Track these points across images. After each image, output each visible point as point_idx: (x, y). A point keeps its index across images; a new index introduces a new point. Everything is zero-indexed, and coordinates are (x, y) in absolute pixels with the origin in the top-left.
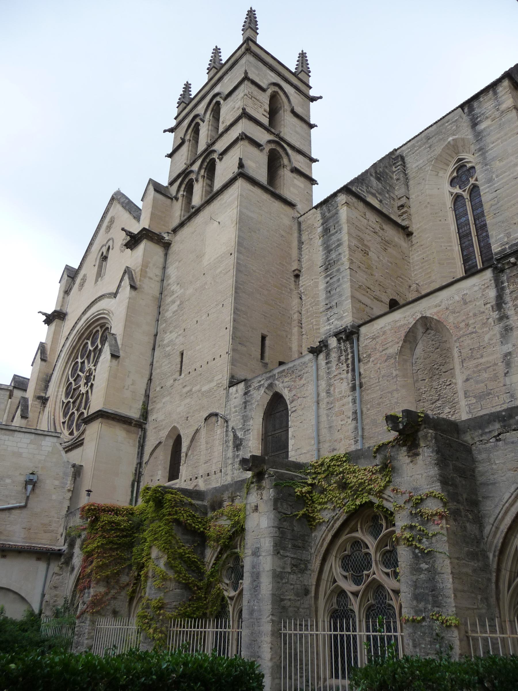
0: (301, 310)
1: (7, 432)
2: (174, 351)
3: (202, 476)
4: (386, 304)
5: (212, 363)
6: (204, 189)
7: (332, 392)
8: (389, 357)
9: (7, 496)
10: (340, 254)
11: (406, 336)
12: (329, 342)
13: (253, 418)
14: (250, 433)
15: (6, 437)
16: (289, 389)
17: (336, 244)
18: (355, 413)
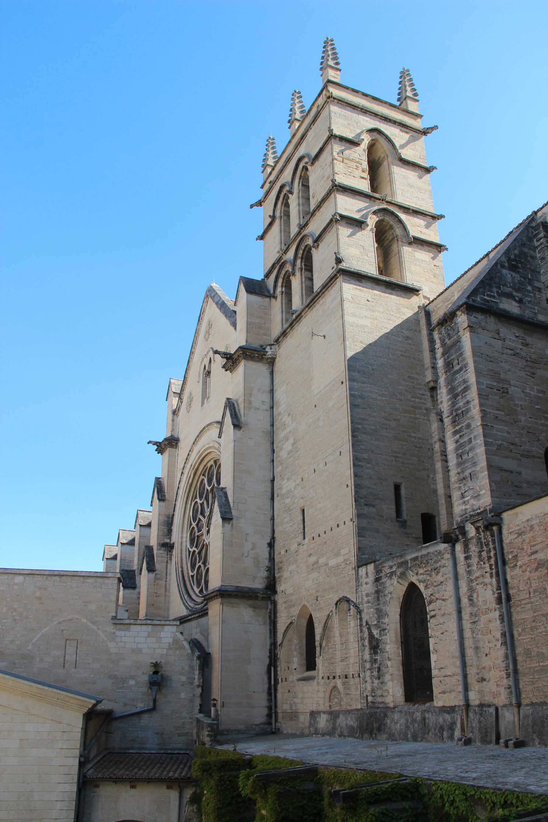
0: (444, 436)
1: (122, 627)
2: (295, 505)
4: (540, 458)
5: (336, 530)
6: (304, 285)
7: (475, 600)
9: (133, 700)
10: (468, 402)
12: (466, 528)
13: (388, 615)
14: (386, 635)
15: (122, 633)
16: (425, 584)
17: (463, 387)
18: (503, 635)
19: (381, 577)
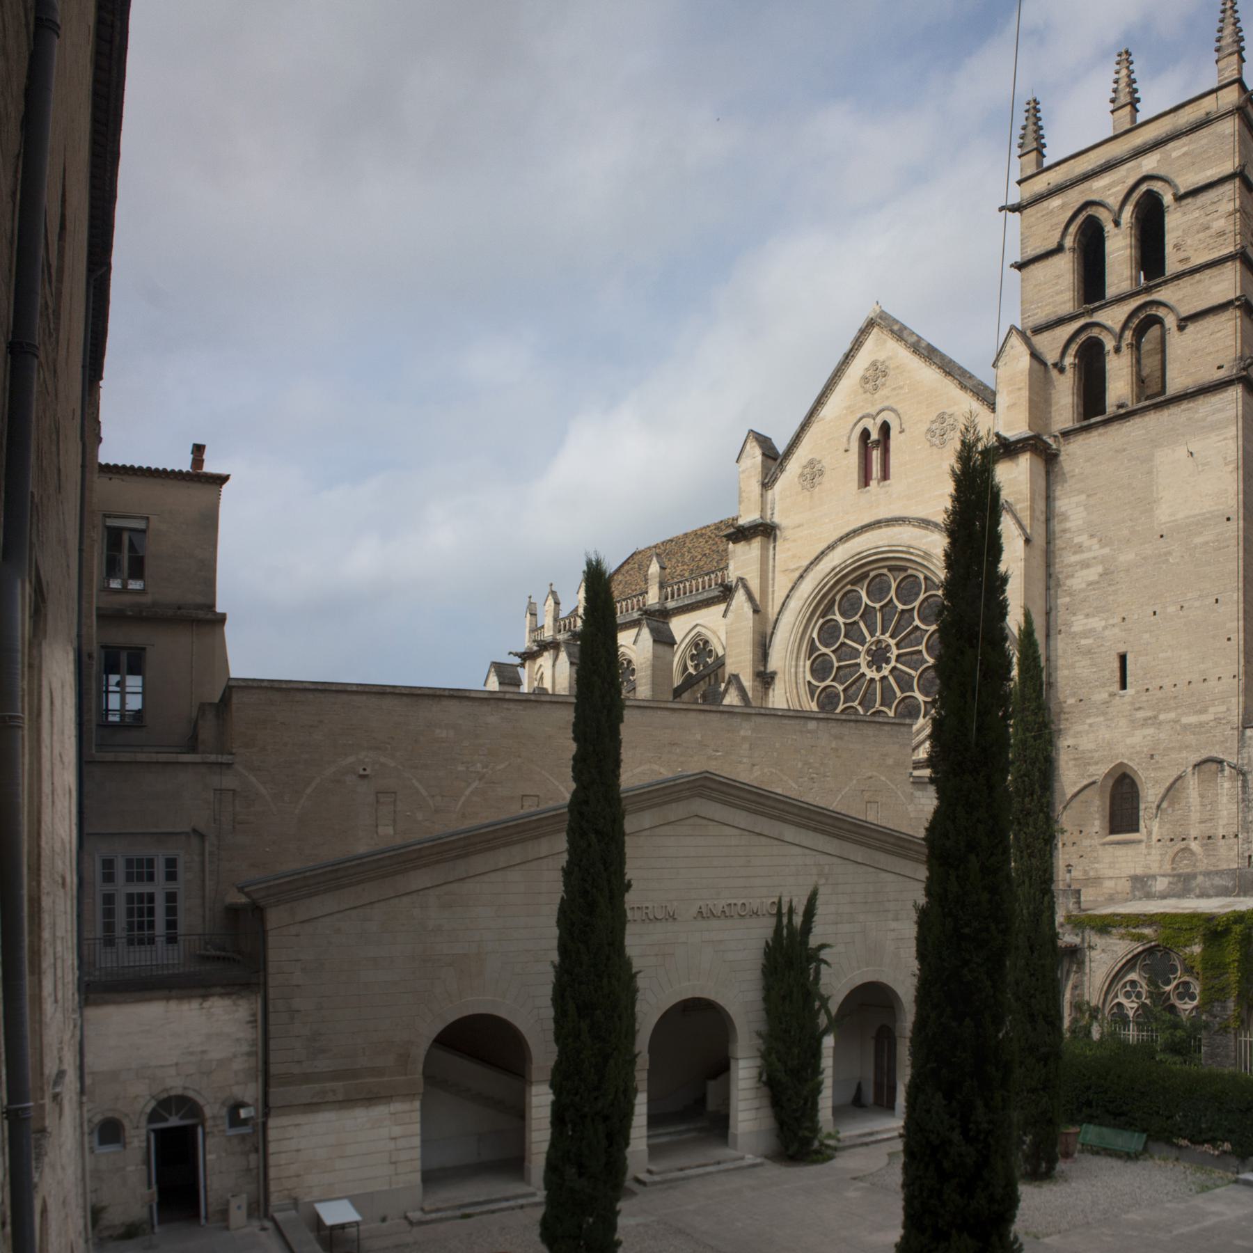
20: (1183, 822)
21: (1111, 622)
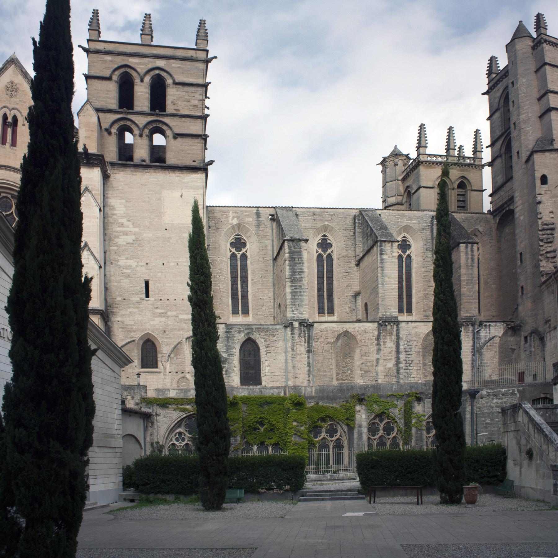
3: (189, 372)
8: (329, 343)
11: (338, 336)
18: (309, 363)
19: (231, 332)
20: (182, 364)
21: (140, 264)
